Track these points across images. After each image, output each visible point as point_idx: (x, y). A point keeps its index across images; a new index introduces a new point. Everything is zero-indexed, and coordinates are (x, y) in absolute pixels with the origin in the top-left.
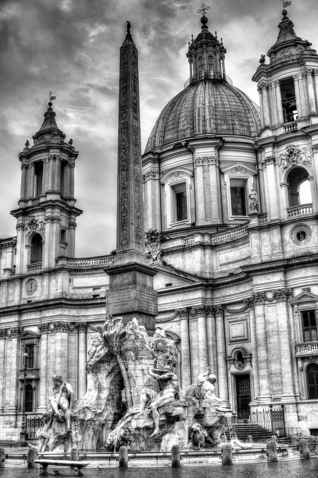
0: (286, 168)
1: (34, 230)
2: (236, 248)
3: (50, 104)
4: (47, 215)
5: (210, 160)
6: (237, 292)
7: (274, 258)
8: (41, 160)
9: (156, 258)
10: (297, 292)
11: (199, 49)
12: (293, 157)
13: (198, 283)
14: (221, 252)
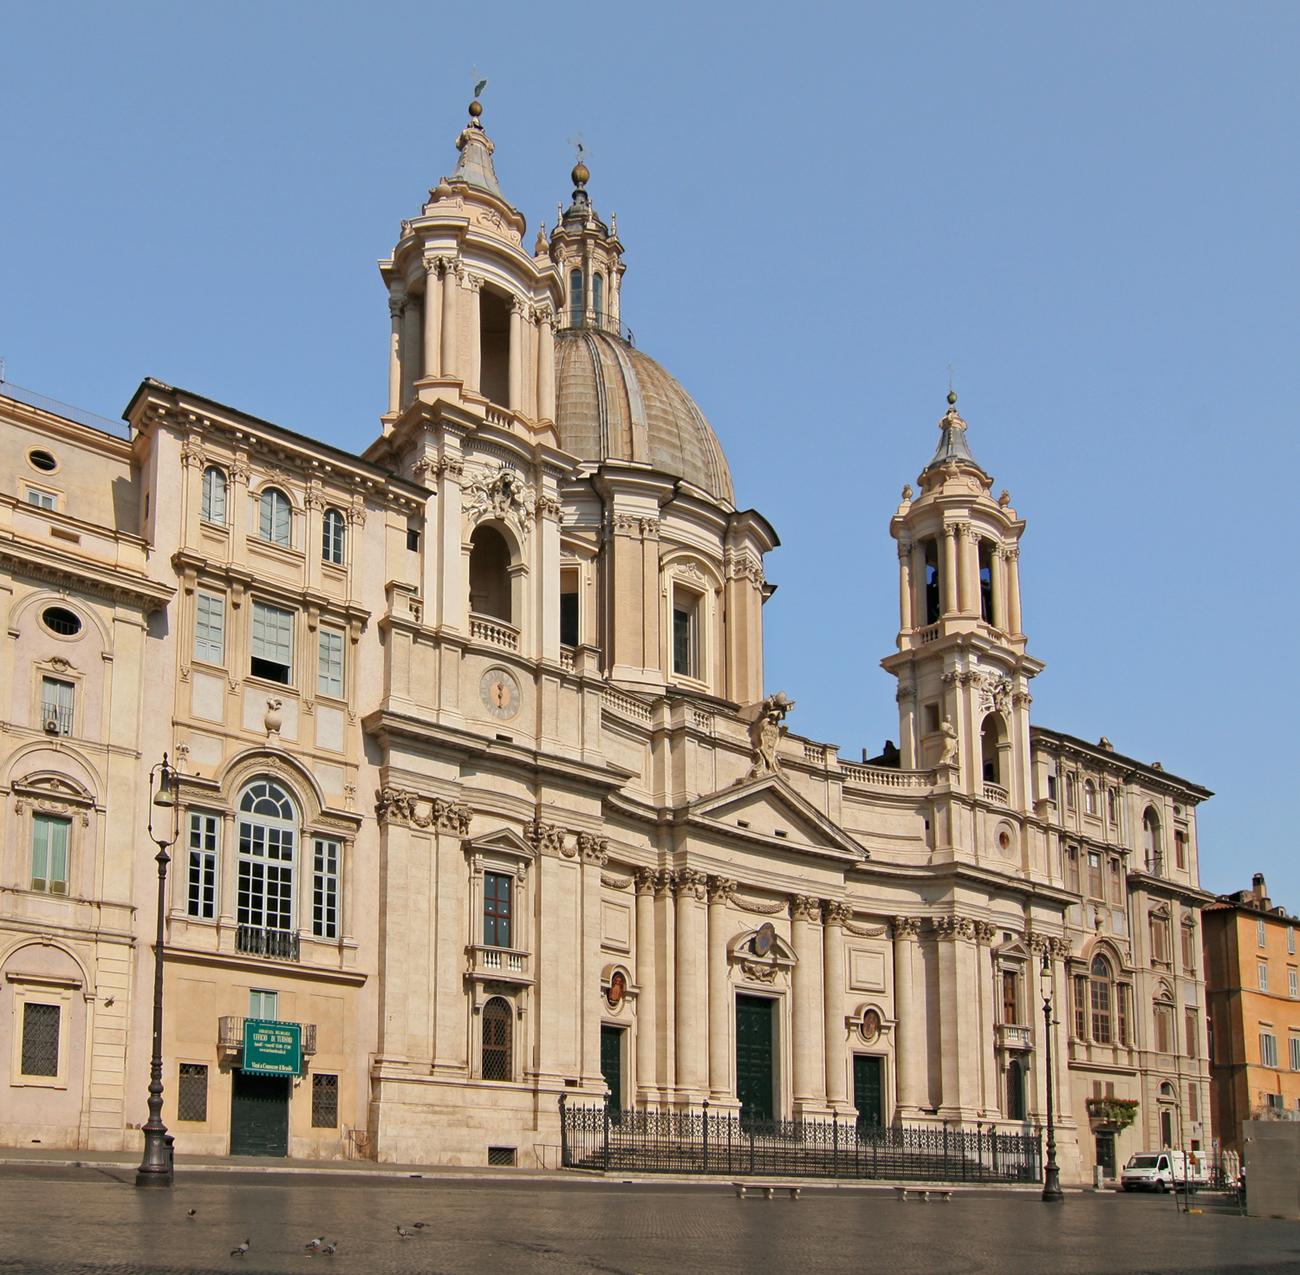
0: (988, 708)
7: (983, 865)
10: (998, 939)
11: (600, 251)
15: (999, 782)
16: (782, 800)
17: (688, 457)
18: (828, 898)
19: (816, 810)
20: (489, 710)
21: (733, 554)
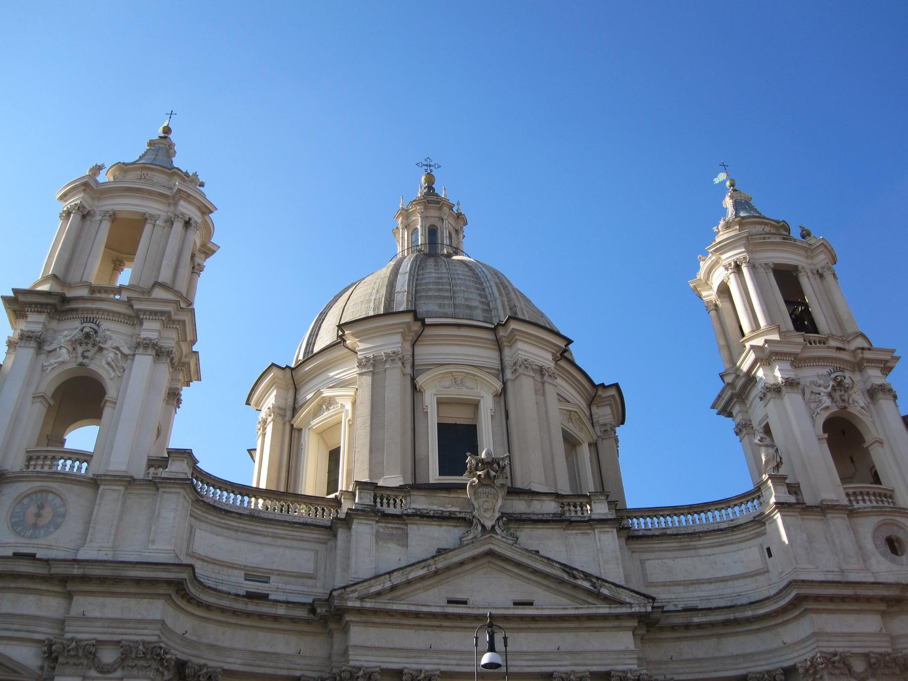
0: (827, 408)
1: (86, 361)
2: (692, 552)
3: (167, 130)
4: (144, 335)
5: (547, 374)
6: (717, 654)
8: (145, 214)
9: (493, 527)
11: (433, 211)
12: (843, 393)
13: (636, 609)
14: (645, 556)
15: (880, 483)
16: (518, 565)
17: (460, 300)
18: (607, 668)
19: (560, 563)
20: (18, 534)
21: (508, 360)
